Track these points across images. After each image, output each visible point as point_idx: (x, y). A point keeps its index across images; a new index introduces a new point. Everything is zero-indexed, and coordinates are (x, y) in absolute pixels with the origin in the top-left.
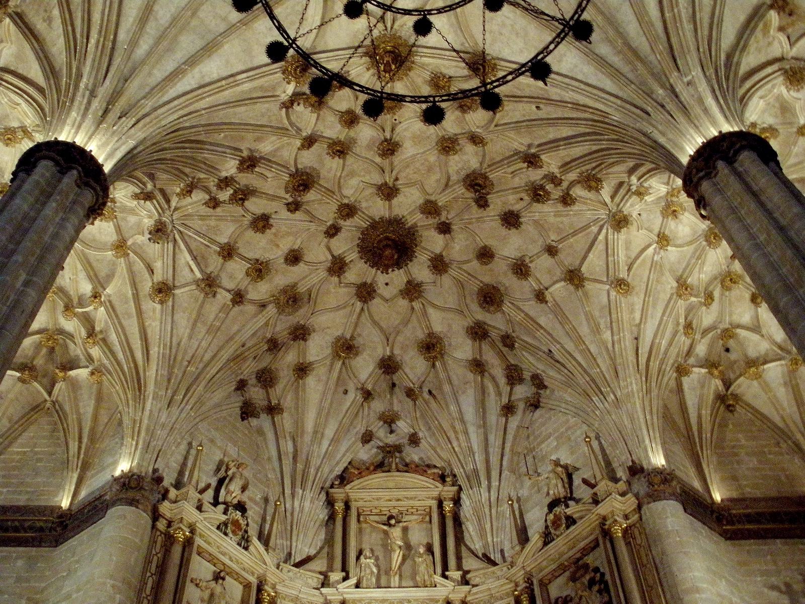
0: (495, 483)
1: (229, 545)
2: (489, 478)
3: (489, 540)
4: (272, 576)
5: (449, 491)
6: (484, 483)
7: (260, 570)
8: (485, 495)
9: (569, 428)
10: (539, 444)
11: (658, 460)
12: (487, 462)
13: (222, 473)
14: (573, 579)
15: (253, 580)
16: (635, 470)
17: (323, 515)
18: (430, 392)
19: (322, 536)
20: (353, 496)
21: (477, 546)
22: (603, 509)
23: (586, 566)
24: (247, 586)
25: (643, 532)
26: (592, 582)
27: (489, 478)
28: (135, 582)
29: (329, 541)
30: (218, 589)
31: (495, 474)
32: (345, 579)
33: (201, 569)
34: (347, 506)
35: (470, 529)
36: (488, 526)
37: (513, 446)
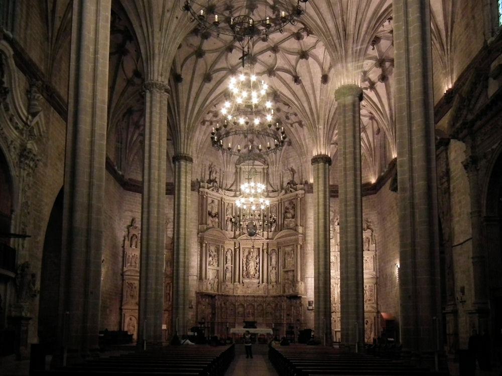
0: (277, 165)
1: (214, 193)
4: (224, 197)
5: (266, 167)
6: (275, 166)
7: (221, 196)
11: (311, 181)
12: (276, 159)
13: (210, 170)
14: (290, 204)
15: (220, 199)
16: (306, 183)
17: (234, 171)
19: (234, 178)
21: (272, 182)
22: (297, 192)
23: (292, 202)
24: (219, 201)
26: (293, 207)
28: (197, 210)
31: (278, 162)
33: (209, 201)
34: (240, 168)
35: (271, 176)
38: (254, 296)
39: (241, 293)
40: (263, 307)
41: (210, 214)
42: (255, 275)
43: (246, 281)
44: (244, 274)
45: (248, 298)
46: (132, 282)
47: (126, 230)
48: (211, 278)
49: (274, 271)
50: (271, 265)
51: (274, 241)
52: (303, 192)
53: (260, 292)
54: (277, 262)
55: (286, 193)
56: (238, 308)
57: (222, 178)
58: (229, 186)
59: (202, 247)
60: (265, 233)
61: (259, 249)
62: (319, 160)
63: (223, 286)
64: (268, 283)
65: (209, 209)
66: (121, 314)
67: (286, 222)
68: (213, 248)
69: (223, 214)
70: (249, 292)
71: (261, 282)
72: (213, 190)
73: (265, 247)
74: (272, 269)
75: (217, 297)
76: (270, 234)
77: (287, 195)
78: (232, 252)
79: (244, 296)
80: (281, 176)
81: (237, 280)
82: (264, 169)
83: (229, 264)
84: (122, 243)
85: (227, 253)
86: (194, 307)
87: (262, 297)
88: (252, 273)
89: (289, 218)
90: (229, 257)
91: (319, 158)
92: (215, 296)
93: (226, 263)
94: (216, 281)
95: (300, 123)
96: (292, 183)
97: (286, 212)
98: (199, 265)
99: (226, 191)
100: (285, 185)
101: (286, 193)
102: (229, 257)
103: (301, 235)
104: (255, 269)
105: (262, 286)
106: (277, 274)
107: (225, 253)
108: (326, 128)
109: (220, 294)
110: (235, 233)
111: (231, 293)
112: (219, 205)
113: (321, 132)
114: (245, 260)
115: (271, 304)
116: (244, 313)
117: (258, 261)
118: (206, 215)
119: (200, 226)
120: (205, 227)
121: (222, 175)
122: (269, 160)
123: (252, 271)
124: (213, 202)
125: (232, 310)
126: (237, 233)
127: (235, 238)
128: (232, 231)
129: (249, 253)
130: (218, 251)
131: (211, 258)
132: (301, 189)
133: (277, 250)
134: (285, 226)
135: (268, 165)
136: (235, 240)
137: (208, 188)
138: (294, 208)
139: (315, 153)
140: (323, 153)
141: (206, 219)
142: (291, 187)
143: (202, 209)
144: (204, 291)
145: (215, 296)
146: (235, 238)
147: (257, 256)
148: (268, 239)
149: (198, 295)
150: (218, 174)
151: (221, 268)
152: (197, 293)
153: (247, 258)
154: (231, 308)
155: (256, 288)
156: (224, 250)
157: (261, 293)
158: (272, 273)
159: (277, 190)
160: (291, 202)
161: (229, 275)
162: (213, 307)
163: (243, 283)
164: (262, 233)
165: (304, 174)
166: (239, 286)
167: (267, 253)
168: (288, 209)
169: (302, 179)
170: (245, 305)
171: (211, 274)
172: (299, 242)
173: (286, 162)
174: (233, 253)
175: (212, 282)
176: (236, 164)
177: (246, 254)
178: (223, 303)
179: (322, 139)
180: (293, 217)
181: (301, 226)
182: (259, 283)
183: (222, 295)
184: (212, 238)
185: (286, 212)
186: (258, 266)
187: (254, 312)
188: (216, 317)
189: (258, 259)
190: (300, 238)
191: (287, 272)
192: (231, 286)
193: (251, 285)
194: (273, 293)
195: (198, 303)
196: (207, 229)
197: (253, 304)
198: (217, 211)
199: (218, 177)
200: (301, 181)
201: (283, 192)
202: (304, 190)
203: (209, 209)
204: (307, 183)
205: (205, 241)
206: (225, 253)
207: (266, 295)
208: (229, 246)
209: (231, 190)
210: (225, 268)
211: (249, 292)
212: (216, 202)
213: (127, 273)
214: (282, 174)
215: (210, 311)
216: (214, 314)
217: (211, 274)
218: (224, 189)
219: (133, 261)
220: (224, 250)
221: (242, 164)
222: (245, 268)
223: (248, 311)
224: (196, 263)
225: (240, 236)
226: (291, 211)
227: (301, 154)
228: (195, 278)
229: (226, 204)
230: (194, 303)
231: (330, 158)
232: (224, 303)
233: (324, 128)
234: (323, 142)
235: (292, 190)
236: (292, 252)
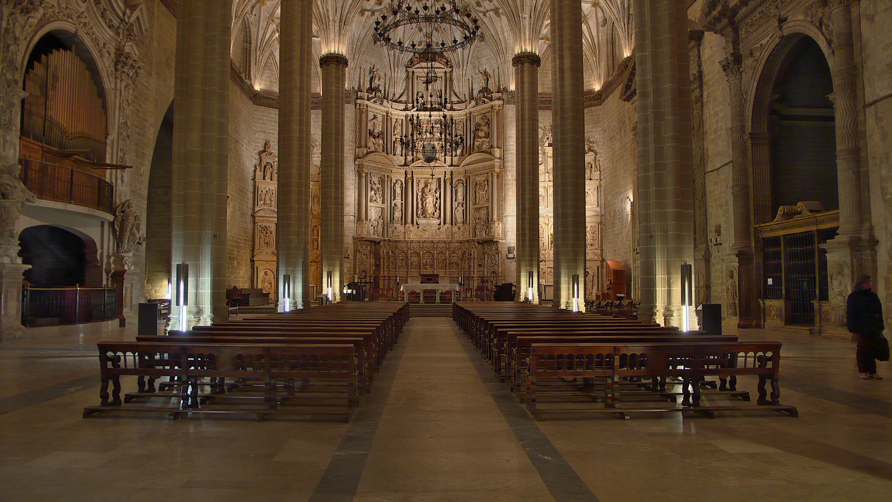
0: (465, 68)
1: (378, 106)
2: (463, 67)
3: (461, 90)
4: (390, 110)
5: (449, 70)
6: (461, 68)
8: (461, 73)
9: (491, 58)
10: (482, 58)
15: (385, 114)
16: (505, 90)
17: (404, 76)
18: (444, 29)
20: (415, 70)
21: (457, 91)
22: (493, 103)
23: (486, 116)
24: (383, 116)
25: (503, 113)
27: (463, 67)
29: (407, 88)
30: (376, 122)
31: (465, 64)
32: (413, 107)
33: (371, 116)
34: (413, 72)
35: (455, 82)
36: (461, 84)
37: (473, 53)
38: (432, 242)
39: (416, 237)
40: (445, 255)
41: (371, 133)
42: (434, 214)
43: (422, 221)
44: (419, 212)
46: (267, 225)
47: (257, 157)
48: (373, 219)
49: (460, 209)
50: (456, 201)
51: (461, 169)
52: (501, 102)
53: (441, 236)
54: (465, 197)
55: (477, 104)
57: (387, 86)
58: (397, 96)
59: (360, 177)
60: (448, 158)
61: (439, 179)
62: (522, 59)
63: (390, 230)
64: (452, 225)
65: (370, 127)
66: (253, 268)
67: (476, 143)
68: (375, 179)
69: (389, 133)
70: (427, 236)
71: (442, 223)
72: (375, 102)
73: (448, 176)
74: (458, 206)
75: (381, 244)
76: (455, 159)
77: (478, 108)
78: (402, 184)
79: (418, 242)
80: (470, 82)
81: (409, 220)
82: (446, 72)
83: (398, 201)
84: (252, 174)
85: (395, 184)
86: (350, 257)
88: (430, 212)
89: (481, 138)
90: (398, 191)
91: (523, 57)
92: (379, 242)
93: (394, 199)
94: (380, 223)
95: (496, 11)
96: (485, 90)
97: (477, 130)
98: (357, 202)
99: (394, 103)
100: (475, 93)
101: (477, 104)
102: (398, 191)
103: (498, 160)
104: (435, 205)
105: (444, 228)
106: (465, 213)
107: (393, 184)
108: (533, 17)
109: (386, 239)
110: (406, 159)
111: (401, 238)
112: (383, 121)
113: (527, 22)
114: (420, 194)
116: (420, 263)
117: (438, 195)
118: (366, 135)
119: (357, 149)
120: (365, 152)
121: (387, 82)
122: (453, 61)
123: (430, 209)
124: (375, 117)
126: (410, 158)
127: (406, 165)
128: (402, 156)
129: (426, 186)
130: (382, 181)
131: (373, 193)
132: (499, 99)
133: (465, 181)
134: (476, 148)
135: (451, 67)
136: (407, 167)
137: (369, 99)
138: (488, 124)
139: (517, 51)
140: (529, 49)
141: (366, 142)
142: (484, 97)
143: (360, 128)
144: (364, 236)
145: (379, 242)
146: (406, 165)
147: (436, 189)
148: (452, 165)
149: (357, 241)
150: (382, 80)
151: (386, 206)
152: (354, 238)
153: (423, 192)
154: (401, 258)
156: (391, 183)
157: (443, 237)
159: (464, 100)
160: (484, 116)
161: (398, 214)
162: (377, 257)
163: (417, 224)
164: (443, 158)
165: (502, 79)
166: (411, 229)
167: (451, 184)
168: (480, 125)
169: (499, 85)
170: (421, 253)
171: (373, 213)
172: (496, 169)
173: (477, 64)
174: (404, 185)
175: (375, 224)
176: (407, 67)
177: (422, 185)
178: (390, 250)
179: (527, 33)
180: (487, 136)
181: (498, 147)
182: (440, 224)
184: (375, 165)
185: (477, 130)
186: (439, 202)
187: (433, 262)
188: (382, 269)
189: (438, 193)
190: (497, 165)
191: (478, 210)
192: (401, 228)
193: (428, 228)
194: (458, 237)
195: (356, 251)
196: (368, 153)
198: (381, 130)
199: (382, 84)
200: (499, 87)
201: (473, 103)
202: (503, 100)
203: (370, 127)
204: (507, 91)
205: (364, 169)
206: (393, 184)
207: (450, 240)
208: (399, 176)
209: (401, 102)
210: (393, 205)
211: (426, 236)
212: (380, 118)
213: (259, 215)
214: (470, 79)
215: (373, 261)
216: (378, 266)
217: (373, 213)
218: (391, 101)
219: (267, 198)
220: (391, 183)
221: (416, 66)
222: (420, 205)
223: (425, 261)
224: (353, 199)
225: (413, 162)
226: (485, 129)
227: (499, 52)
228: (352, 218)
229: (394, 121)
230: (351, 252)
231: (538, 57)
232: (392, 252)
233: (530, 17)
234: (529, 35)
235: (485, 100)
236: (486, 182)
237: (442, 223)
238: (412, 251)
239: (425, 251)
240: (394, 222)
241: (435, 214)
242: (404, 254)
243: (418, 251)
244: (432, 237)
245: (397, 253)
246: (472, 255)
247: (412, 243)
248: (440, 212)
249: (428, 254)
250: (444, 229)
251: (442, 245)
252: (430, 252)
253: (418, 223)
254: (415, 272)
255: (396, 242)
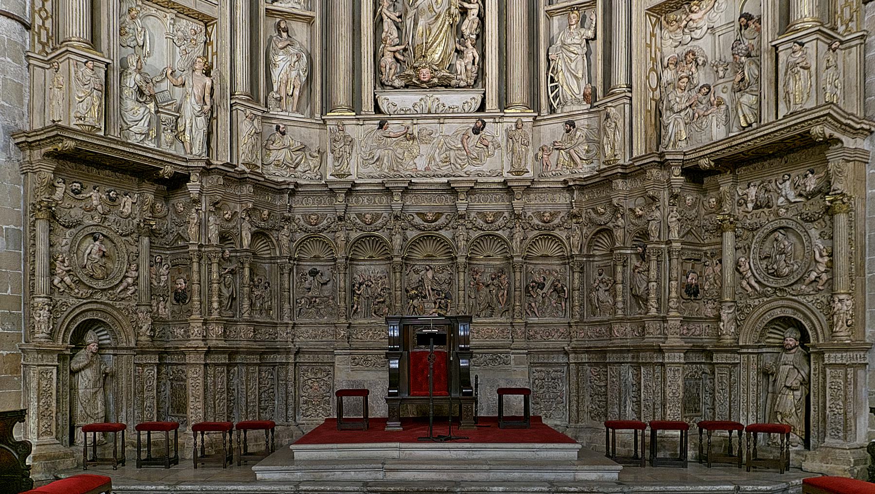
39: (372, 169)
44: (388, 60)
45: (410, 200)
53: (489, 165)
56: (351, 261)
63: (245, 128)
70: (421, 164)
71: (492, 105)
81: (341, 94)
87: (507, 188)
115: (562, 235)
125: (314, 273)
155: (465, 137)
158: (563, 44)
163: (377, 109)
166: (353, 130)
183: (242, 180)
197: (446, 234)
223: (415, 277)
237: (492, 105)
238: (354, 235)
239: (412, 234)
240: (272, 103)
241: (460, 65)
242: (315, 250)
243: (383, 234)
244: (445, 170)
245: (285, 241)
246: (654, 237)
247: (353, 200)
248: (483, 56)
249: (429, 248)
250: (509, 123)
251: (494, 205)
252: (441, 240)
253: (384, 107)
254: (369, 327)
255: (278, 189)
